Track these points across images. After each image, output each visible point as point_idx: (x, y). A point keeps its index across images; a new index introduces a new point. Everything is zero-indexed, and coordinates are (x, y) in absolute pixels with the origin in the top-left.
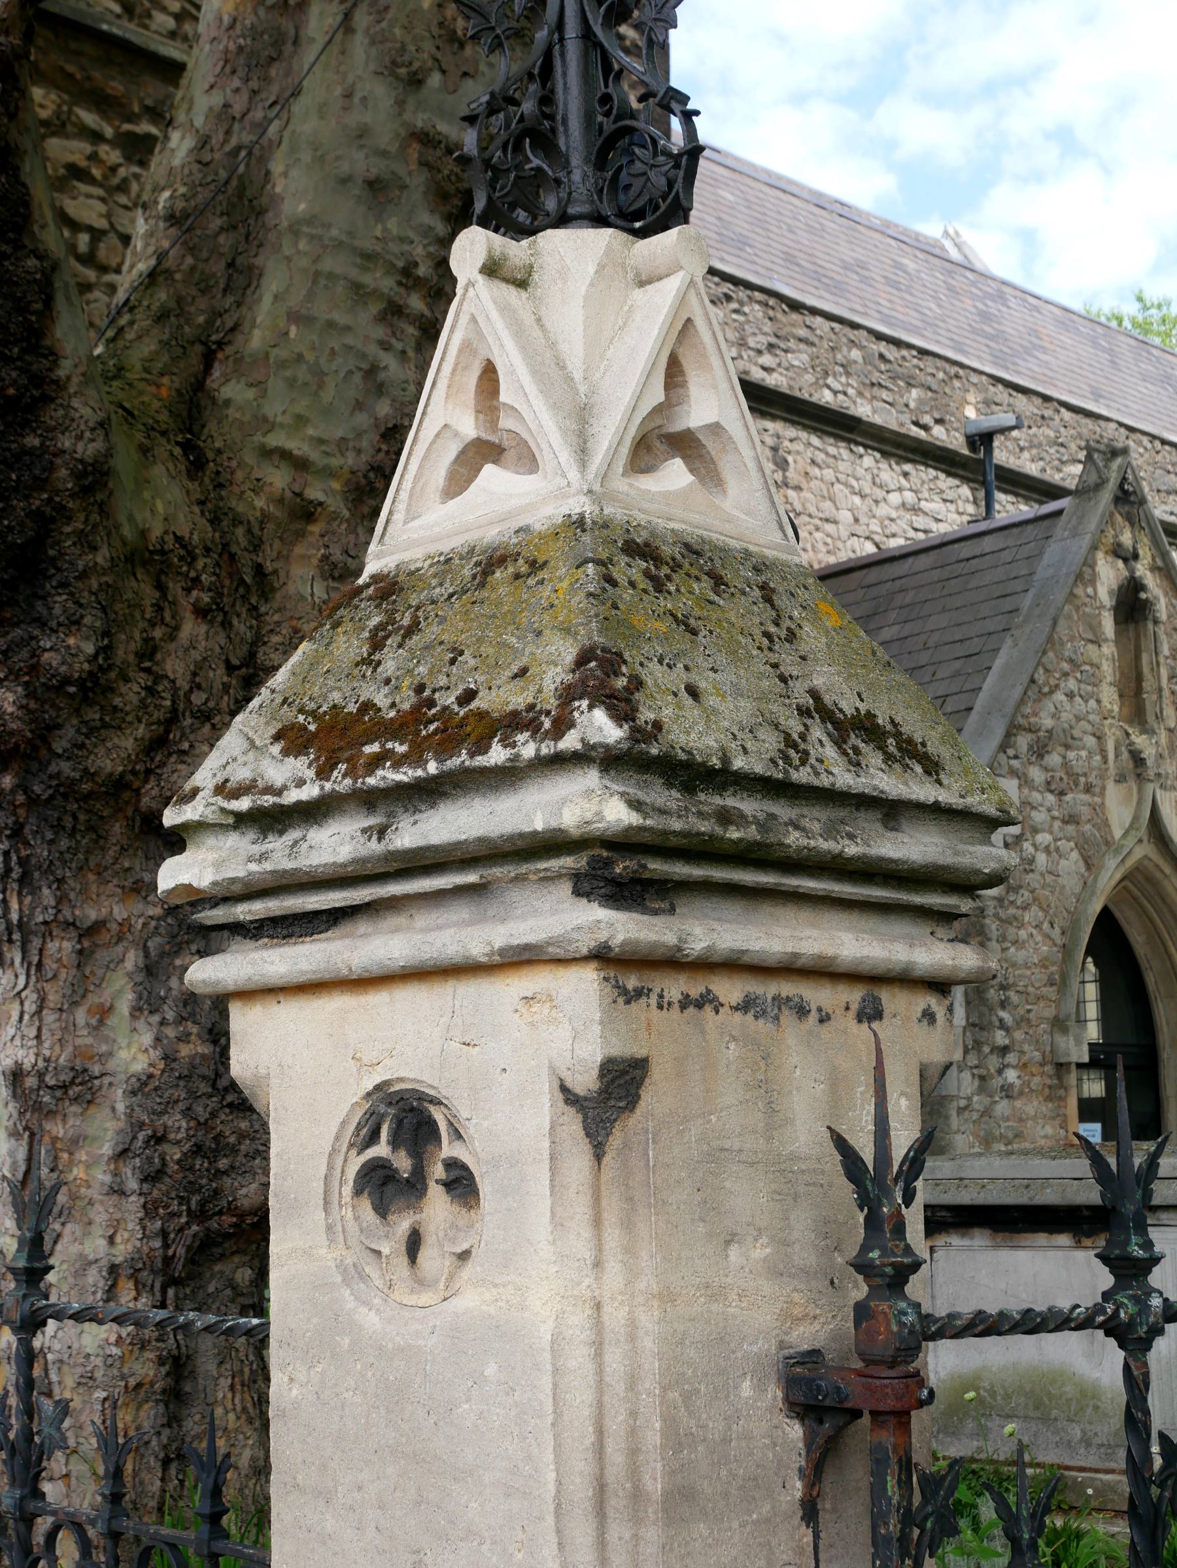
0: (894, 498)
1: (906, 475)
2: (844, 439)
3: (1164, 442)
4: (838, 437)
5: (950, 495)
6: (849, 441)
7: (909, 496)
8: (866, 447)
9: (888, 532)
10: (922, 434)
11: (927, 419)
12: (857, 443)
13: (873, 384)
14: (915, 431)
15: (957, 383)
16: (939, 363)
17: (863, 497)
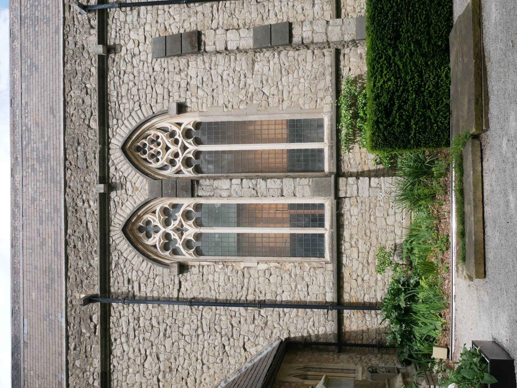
0: (126, 348)
1: (115, 340)
2: (110, 377)
3: (66, 159)
4: (110, 381)
5: (118, 314)
6: (110, 373)
7: (123, 339)
8: (110, 364)
9: (139, 354)
10: (98, 327)
11: (92, 326)
12: (110, 369)
13: (86, 356)
14: (98, 333)
15: (74, 303)
16: (69, 314)
17: (129, 367)
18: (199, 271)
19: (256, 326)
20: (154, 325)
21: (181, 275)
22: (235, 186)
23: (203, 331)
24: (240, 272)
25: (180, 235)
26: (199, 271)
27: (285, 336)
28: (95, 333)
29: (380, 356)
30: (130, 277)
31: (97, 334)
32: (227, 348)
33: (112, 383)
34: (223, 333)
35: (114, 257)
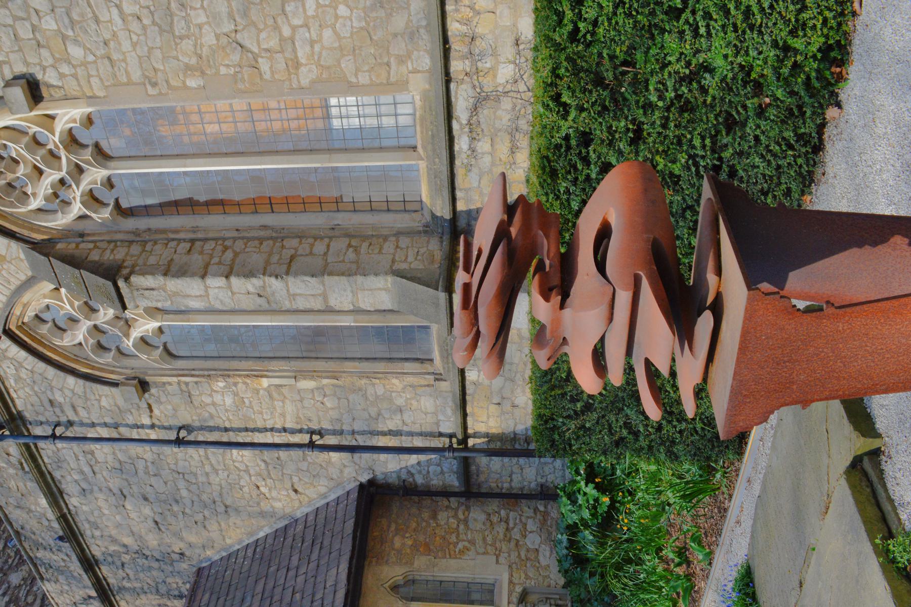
18: (181, 390)
19: (310, 463)
20: (122, 459)
21: (146, 395)
22: (216, 291)
23: (214, 468)
24: (261, 392)
25: (126, 327)
26: (181, 390)
27: (364, 478)
28: (23, 469)
29: (542, 508)
30: (51, 398)
31: (27, 469)
32: (262, 489)
33: (79, 524)
34: (252, 472)
35: (8, 370)
